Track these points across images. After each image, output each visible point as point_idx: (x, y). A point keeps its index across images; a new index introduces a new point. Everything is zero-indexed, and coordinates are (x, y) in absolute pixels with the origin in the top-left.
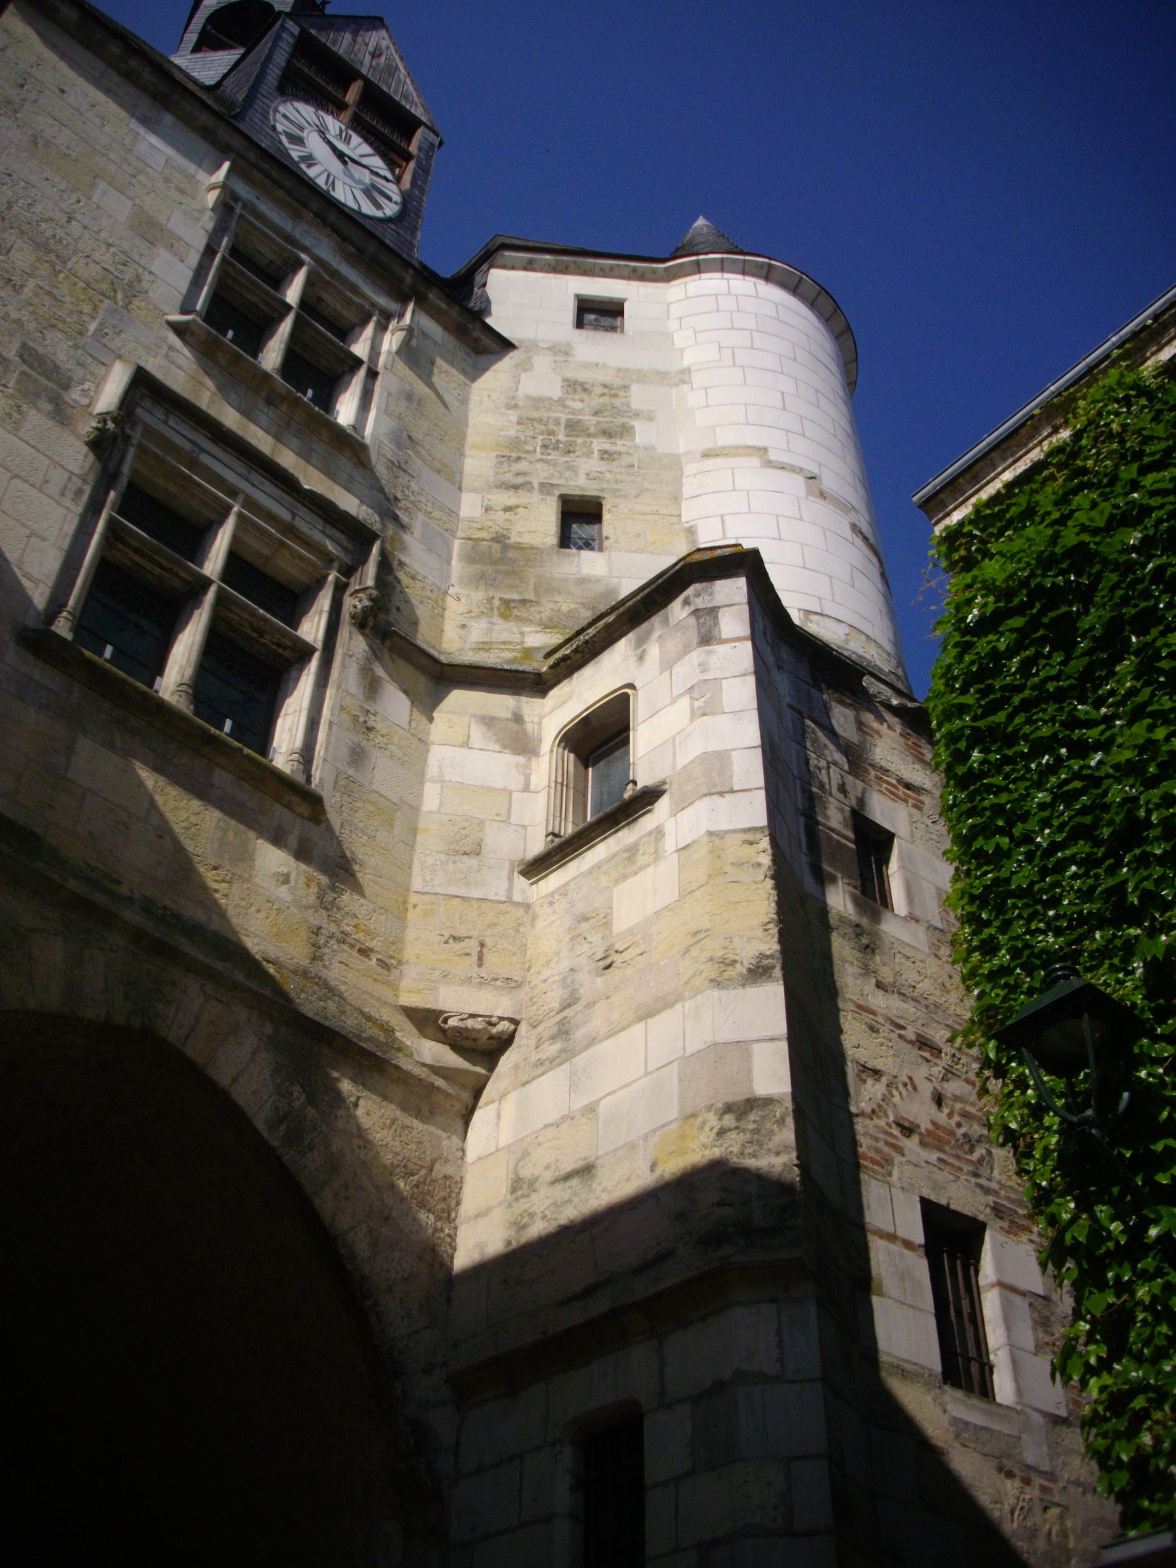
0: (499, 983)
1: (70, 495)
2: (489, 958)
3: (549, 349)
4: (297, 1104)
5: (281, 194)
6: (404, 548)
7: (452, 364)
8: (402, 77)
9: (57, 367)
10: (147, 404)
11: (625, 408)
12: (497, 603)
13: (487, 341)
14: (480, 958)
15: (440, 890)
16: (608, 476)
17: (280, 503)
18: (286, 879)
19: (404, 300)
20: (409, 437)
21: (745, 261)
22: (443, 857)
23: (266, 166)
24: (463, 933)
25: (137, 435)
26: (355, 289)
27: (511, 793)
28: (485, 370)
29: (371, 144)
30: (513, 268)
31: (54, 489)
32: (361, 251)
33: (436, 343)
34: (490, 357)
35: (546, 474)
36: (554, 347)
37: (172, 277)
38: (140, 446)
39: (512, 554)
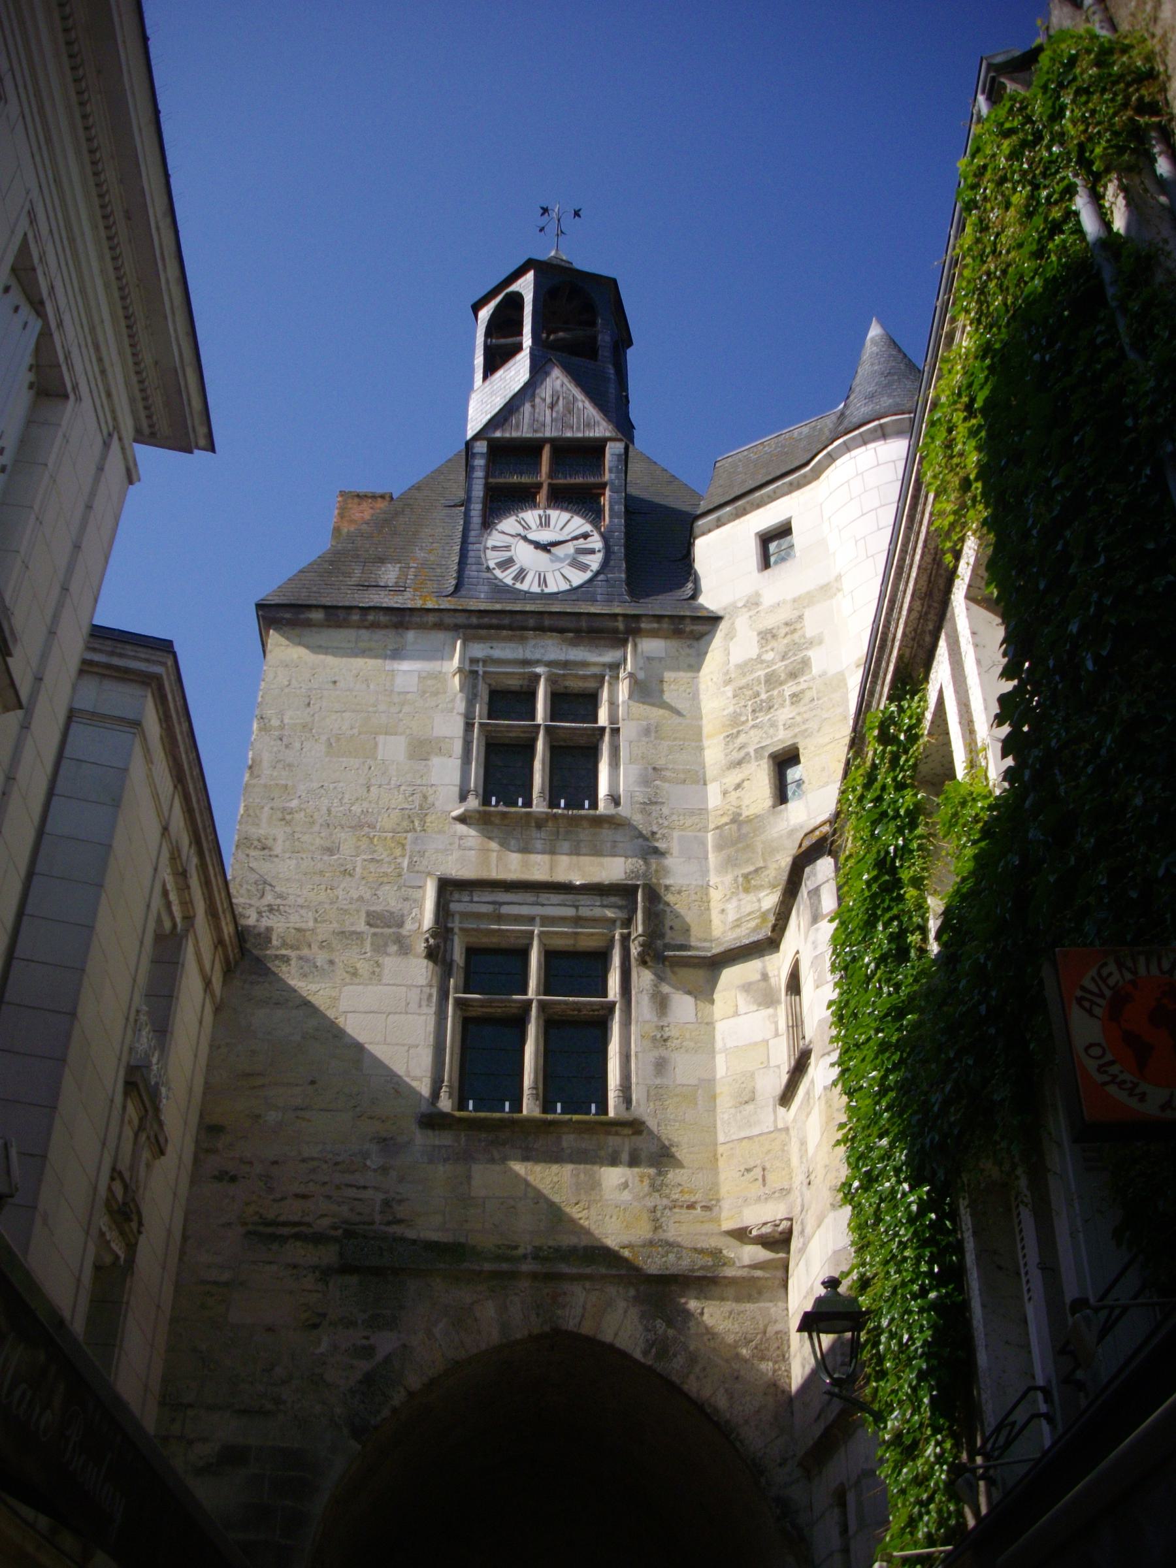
0: (777, 1195)
1: (424, 1003)
2: (770, 1177)
3: (745, 606)
4: (660, 1332)
5: (505, 633)
6: (666, 871)
7: (678, 669)
8: (580, 405)
9: (392, 913)
10: (456, 896)
11: (803, 641)
12: (740, 879)
13: (699, 628)
14: (764, 1180)
15: (734, 1137)
16: (798, 719)
17: (565, 905)
18: (625, 1185)
19: (623, 643)
20: (654, 769)
21: (861, 434)
22: (733, 1111)
23: (486, 620)
24: (752, 1164)
25: (456, 924)
26: (584, 664)
27: (767, 1041)
28: (706, 653)
29: (566, 510)
30: (710, 531)
31: (413, 1006)
32: (577, 631)
33: (660, 659)
34: (707, 637)
35: (756, 739)
36: (747, 602)
37: (448, 775)
38: (461, 929)
39: (745, 830)
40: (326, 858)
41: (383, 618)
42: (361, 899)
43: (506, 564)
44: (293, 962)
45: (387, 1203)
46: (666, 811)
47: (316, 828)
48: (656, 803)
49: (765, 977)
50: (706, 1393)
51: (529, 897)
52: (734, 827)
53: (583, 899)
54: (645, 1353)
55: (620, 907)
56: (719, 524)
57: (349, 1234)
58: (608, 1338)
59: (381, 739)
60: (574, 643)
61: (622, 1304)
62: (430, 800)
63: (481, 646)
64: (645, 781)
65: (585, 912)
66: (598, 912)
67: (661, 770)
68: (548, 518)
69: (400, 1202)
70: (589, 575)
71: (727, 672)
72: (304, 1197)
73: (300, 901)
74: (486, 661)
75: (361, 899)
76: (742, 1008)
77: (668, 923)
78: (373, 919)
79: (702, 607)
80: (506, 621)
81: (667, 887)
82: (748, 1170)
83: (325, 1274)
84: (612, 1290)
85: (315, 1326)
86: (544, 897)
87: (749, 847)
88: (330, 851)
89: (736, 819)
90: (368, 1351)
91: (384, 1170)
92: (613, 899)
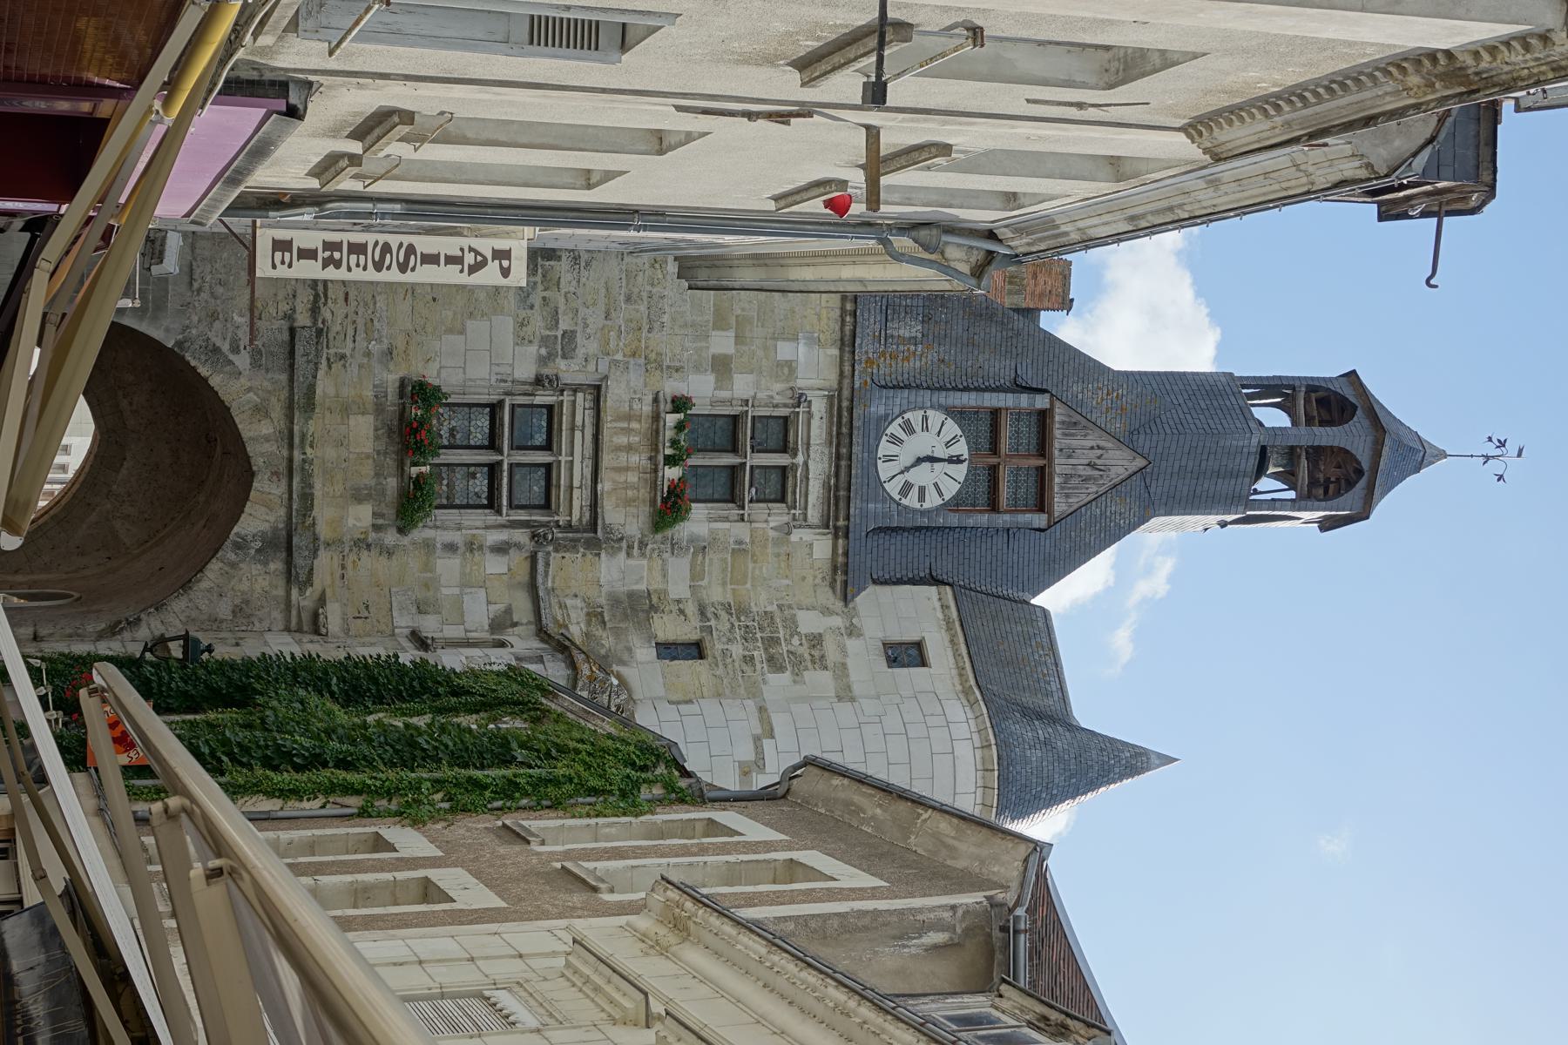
10: (589, 397)
25: (566, 397)
40: (622, 298)
41: (848, 328)
42: (586, 326)
43: (908, 428)
46: (665, 555)
47: (649, 288)
49: (515, 625)
51: (589, 451)
52: (646, 607)
53: (587, 493)
54: (237, 534)
56: (944, 607)
62: (675, 375)
64: (692, 540)
65: (576, 493)
66: (576, 504)
72: (346, 299)
73: (583, 280)
74: (810, 415)
76: (491, 608)
77: (567, 555)
78: (569, 336)
80: (845, 430)
83: (289, 316)
84: (282, 512)
86: (589, 463)
87: (626, 617)
88: (628, 299)
89: (653, 608)
90: (235, 349)
91: (368, 354)
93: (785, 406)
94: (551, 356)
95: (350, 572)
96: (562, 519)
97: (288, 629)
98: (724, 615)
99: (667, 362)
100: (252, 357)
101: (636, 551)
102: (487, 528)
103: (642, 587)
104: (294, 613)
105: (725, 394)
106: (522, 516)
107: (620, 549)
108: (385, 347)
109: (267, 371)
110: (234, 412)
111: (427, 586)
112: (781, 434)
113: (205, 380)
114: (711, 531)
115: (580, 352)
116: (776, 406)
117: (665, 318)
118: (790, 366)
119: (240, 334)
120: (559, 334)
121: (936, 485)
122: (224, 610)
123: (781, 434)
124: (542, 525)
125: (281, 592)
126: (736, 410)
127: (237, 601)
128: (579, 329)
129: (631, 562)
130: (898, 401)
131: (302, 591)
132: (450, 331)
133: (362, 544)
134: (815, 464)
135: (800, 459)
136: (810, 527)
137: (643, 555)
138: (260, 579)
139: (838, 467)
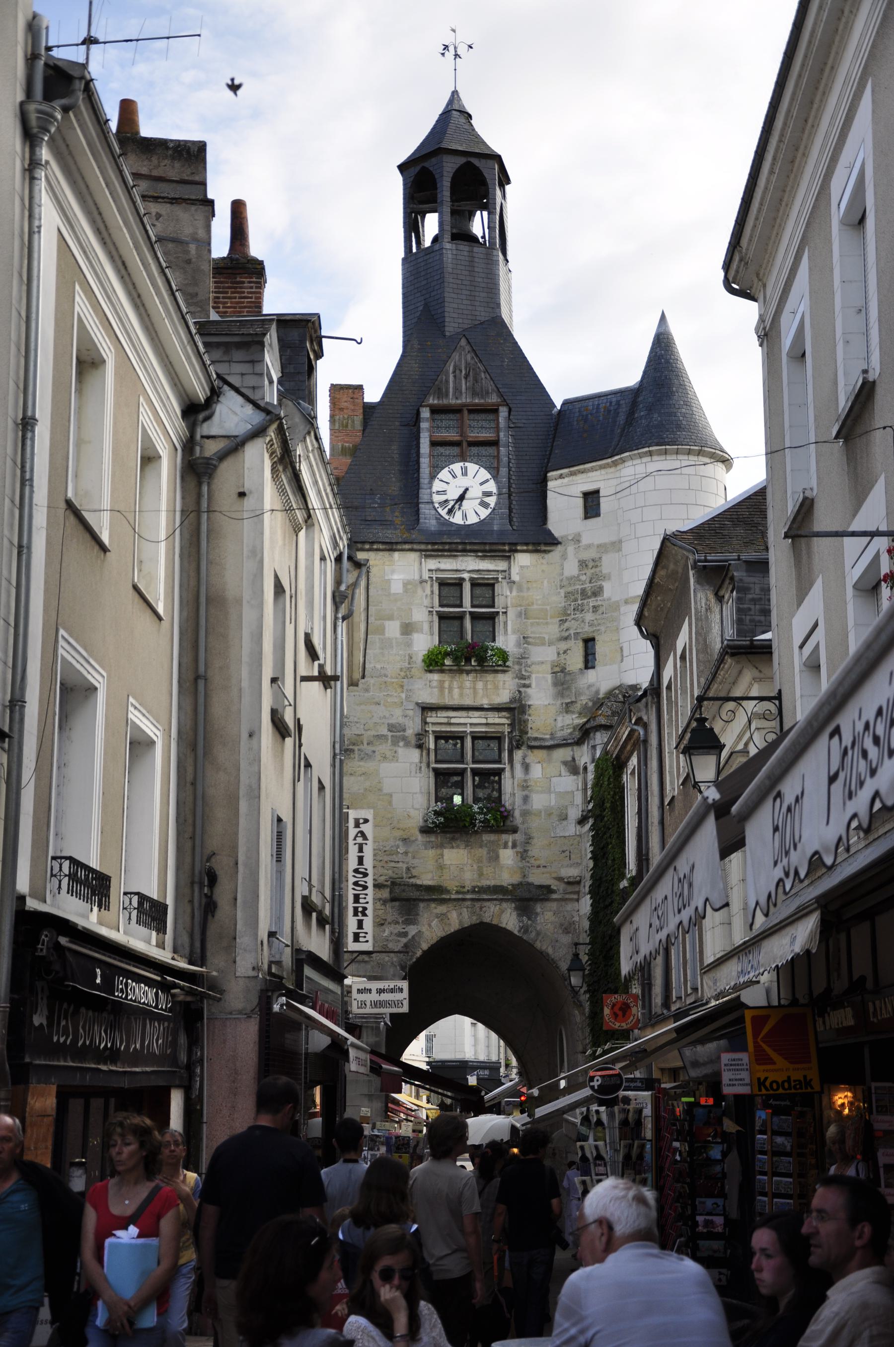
10: (429, 714)
25: (430, 728)
31: (413, 773)
40: (366, 695)
41: (381, 547)
44: (356, 752)
45: (408, 869)
46: (529, 662)
48: (525, 658)
50: (544, 948)
51: (464, 713)
52: (562, 675)
54: (519, 931)
55: (507, 718)
56: (561, 477)
57: (394, 884)
58: (503, 925)
59: (387, 624)
60: (484, 557)
61: (509, 911)
62: (414, 659)
63: (434, 561)
64: (518, 645)
65: (490, 721)
66: (497, 721)
67: (528, 637)
68: (466, 468)
69: (414, 868)
70: (490, 510)
71: (561, 580)
73: (356, 719)
74: (438, 570)
75: (385, 717)
76: (563, 773)
77: (530, 726)
78: (391, 728)
79: (549, 533)
81: (529, 706)
82: (564, 852)
84: (504, 905)
85: (382, 924)
86: (471, 713)
89: (563, 670)
90: (405, 934)
91: (406, 853)
92: (504, 714)
93: (432, 586)
94: (404, 738)
95: (542, 862)
96: (507, 729)
97: (578, 900)
98: (567, 625)
99: (406, 665)
100: (409, 924)
101: (527, 682)
102: (513, 777)
103: (549, 677)
104: (567, 896)
105: (426, 627)
106: (506, 755)
107: (525, 692)
108: (400, 843)
109: (418, 915)
110: (443, 934)
111: (550, 814)
112: (449, 587)
113: (425, 952)
114: (514, 632)
115: (401, 720)
116: (432, 592)
117: (378, 666)
118: (406, 584)
119: (396, 931)
120: (390, 734)
121: (482, 484)
122: (566, 939)
123: (449, 587)
124: (510, 743)
125: (554, 905)
126: (436, 619)
127: (561, 931)
128: (387, 722)
129: (533, 685)
130: (427, 511)
131: (554, 892)
132: (390, 803)
133: (523, 855)
134: (469, 566)
135: (466, 576)
136: (510, 568)
137: (529, 677)
138: (546, 917)
139: (470, 551)
